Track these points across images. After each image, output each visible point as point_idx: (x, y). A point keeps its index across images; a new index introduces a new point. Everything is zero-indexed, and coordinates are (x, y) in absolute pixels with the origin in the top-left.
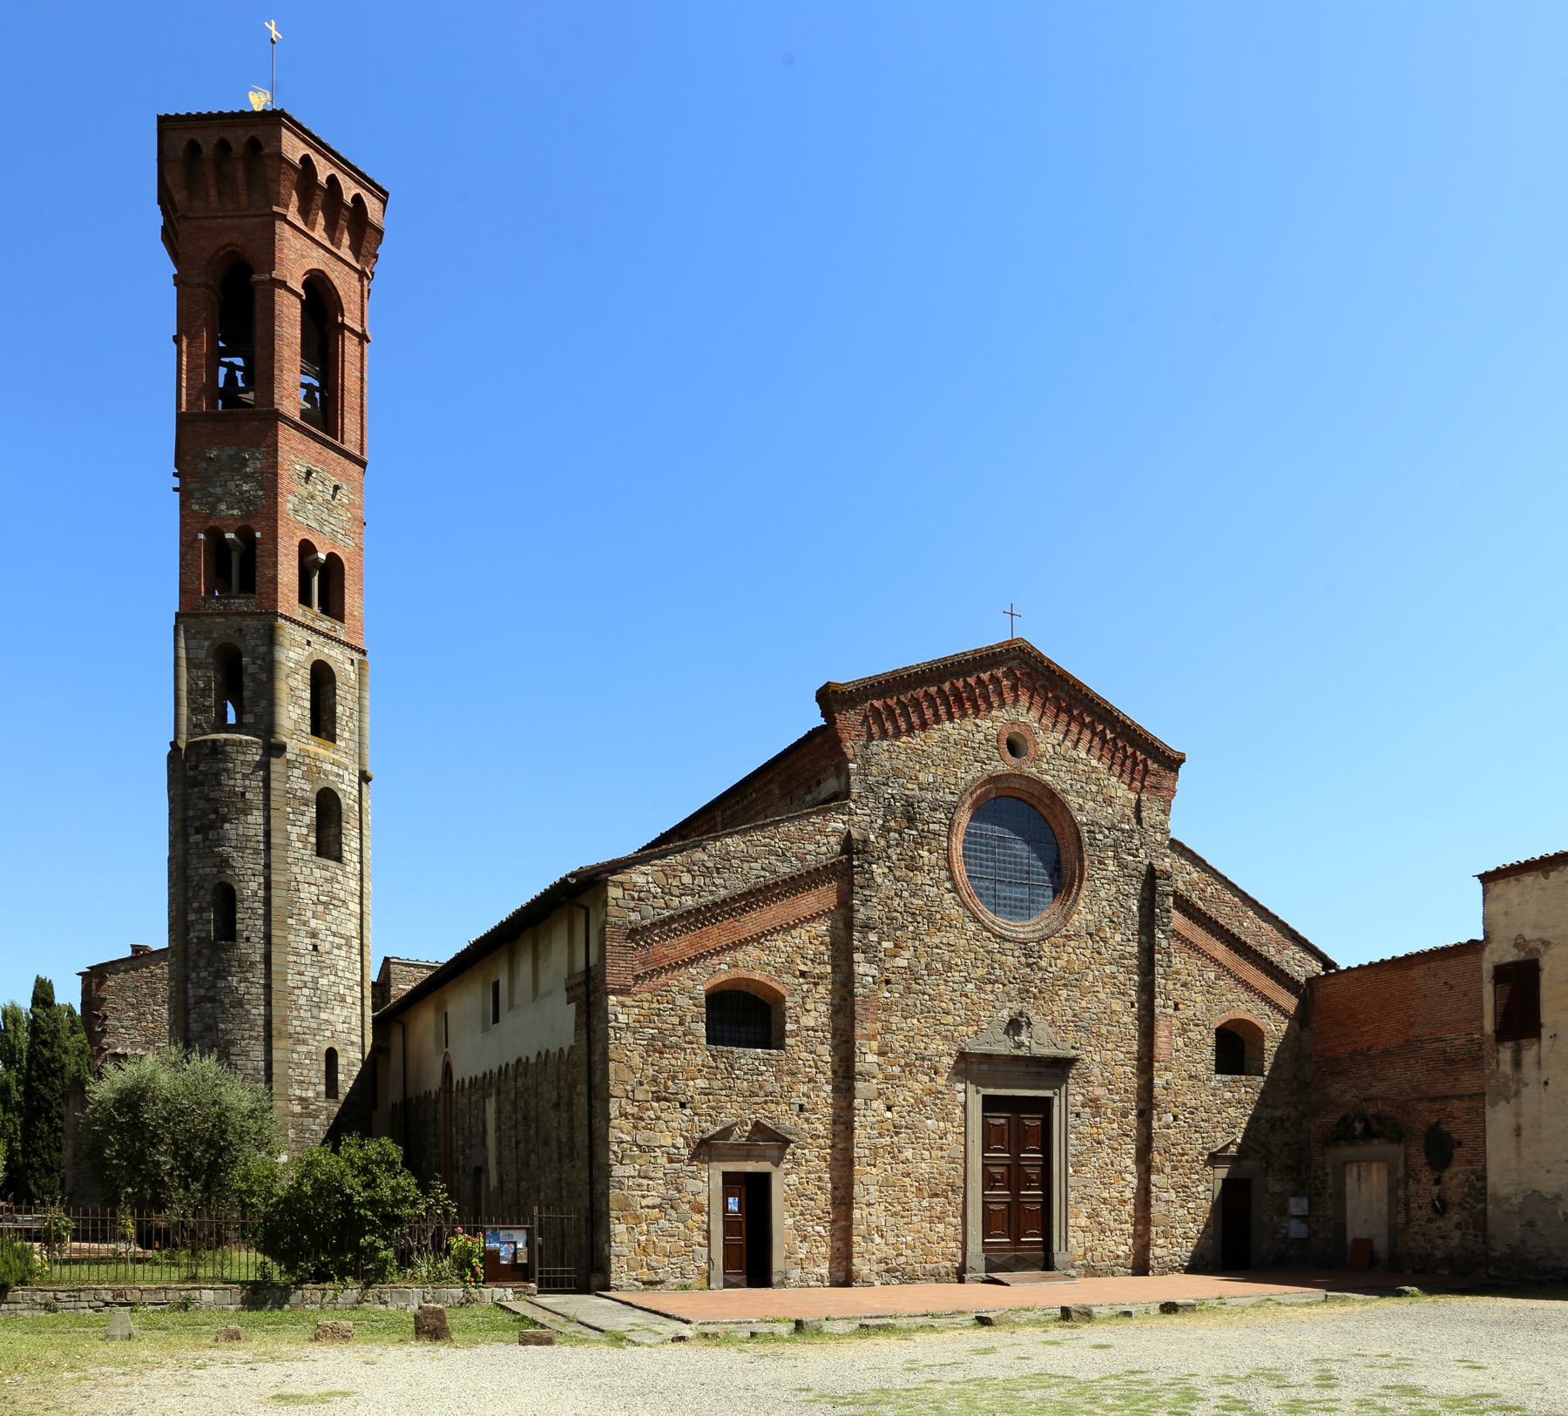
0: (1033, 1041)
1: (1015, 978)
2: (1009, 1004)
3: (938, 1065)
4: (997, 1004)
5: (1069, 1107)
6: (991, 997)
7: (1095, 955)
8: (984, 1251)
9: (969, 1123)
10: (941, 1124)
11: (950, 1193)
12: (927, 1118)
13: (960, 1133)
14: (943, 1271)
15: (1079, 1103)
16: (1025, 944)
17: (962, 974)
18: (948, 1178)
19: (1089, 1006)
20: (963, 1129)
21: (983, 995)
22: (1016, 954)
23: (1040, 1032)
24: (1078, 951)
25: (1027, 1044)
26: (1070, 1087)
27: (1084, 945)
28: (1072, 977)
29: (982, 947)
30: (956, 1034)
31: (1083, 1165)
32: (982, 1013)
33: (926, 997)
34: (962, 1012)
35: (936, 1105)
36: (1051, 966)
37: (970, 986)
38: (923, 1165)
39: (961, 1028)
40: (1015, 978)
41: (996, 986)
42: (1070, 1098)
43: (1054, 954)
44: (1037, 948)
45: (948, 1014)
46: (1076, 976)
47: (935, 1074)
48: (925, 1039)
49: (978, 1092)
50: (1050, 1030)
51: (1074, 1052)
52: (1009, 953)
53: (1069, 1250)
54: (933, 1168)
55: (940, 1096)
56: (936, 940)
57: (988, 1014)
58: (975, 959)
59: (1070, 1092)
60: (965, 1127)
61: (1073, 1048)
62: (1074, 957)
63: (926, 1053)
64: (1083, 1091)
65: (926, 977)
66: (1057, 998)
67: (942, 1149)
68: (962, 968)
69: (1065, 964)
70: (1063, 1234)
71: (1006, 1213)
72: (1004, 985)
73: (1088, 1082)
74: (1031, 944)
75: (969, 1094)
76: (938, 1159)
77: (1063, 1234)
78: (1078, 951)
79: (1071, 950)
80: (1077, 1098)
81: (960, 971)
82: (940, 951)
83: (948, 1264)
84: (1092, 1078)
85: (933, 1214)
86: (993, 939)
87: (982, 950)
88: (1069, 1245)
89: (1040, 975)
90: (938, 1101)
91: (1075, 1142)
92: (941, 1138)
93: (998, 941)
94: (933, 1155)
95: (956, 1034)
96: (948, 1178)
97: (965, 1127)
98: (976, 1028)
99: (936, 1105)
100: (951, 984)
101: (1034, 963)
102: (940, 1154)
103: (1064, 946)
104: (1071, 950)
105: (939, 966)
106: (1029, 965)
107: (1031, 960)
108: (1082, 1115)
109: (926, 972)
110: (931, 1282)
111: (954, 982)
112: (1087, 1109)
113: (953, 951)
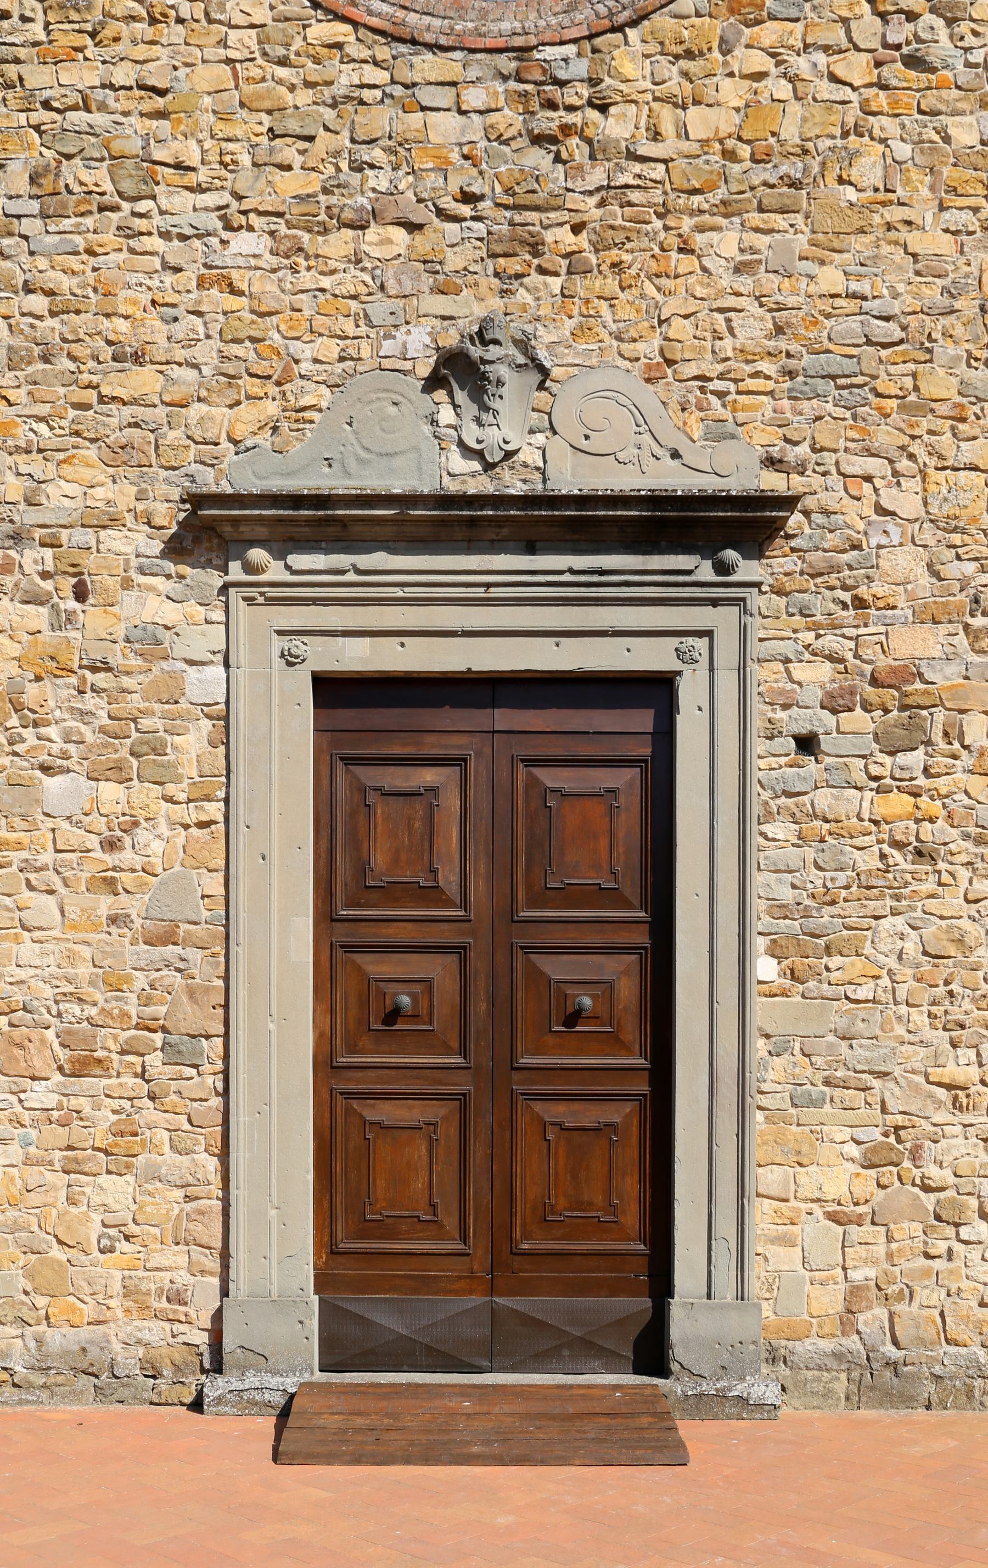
0: (557, 447)
1: (467, 198)
2: (441, 305)
3: (90, 562)
4: (379, 309)
5: (757, 707)
6: (351, 281)
7: (895, 72)
8: (322, 1283)
9: (241, 780)
10: (110, 791)
11: (155, 1060)
12: (46, 769)
13: (202, 825)
14: (128, 1361)
15: (813, 695)
16: (523, 51)
17: (210, 199)
18: (146, 1001)
19: (854, 286)
20: (214, 810)
21: (307, 279)
22: (474, 97)
23: (596, 412)
24: (801, 65)
25: (530, 456)
26: (757, 628)
27: (838, 36)
28: (761, 174)
29: (309, 85)
30: (174, 436)
31: (828, 951)
32: (305, 351)
33: (38, 303)
34: (206, 353)
35: (84, 715)
36: (656, 136)
37: (243, 243)
38: (27, 950)
39: (197, 410)
40: (467, 198)
41: (373, 233)
42: (757, 672)
43: (675, 85)
44: (581, 68)
45: (138, 358)
46: (793, 168)
47: (81, 594)
48: (34, 465)
49: (290, 660)
50: (648, 396)
51: (774, 482)
52: (444, 97)
53: (755, 1287)
54: (72, 958)
55: (101, 679)
56: (88, 77)
57: (331, 348)
58: (273, 134)
59: (755, 649)
60: (227, 801)
61: (771, 462)
62: (783, 90)
63: (31, 517)
64: (830, 642)
65: (31, 226)
66: (686, 263)
67: (110, 885)
68: (202, 176)
69: (726, 122)
70: (726, 1227)
71: (449, 1133)
72: (413, 227)
73: (860, 603)
74: (549, 53)
75: (240, 675)
76: (96, 929)
77: (726, 1227)
78: (801, 65)
79: (760, 61)
80: (799, 672)
81: (199, 189)
82: (99, 119)
83: (155, 1332)
84: (879, 588)
85: (76, 1132)
86: (354, 50)
87: (304, 97)
88: (755, 1269)
89: (597, 176)
90: (90, 701)
91: (792, 855)
92: (111, 845)
93: (383, 53)
94: (73, 912)
95: (174, 436)
96: (146, 1001)
97: (227, 801)
98: (272, 409)
99: (84, 715)
100: (156, 243)
101: (567, 130)
102: (105, 905)
103: (726, 50)
104: (760, 61)
105: (100, 177)
106: (538, 140)
107: (548, 121)
108: (825, 743)
109: (35, 206)
110: (75, 1396)
111: (165, 235)
112: (858, 719)
113: (161, 115)
